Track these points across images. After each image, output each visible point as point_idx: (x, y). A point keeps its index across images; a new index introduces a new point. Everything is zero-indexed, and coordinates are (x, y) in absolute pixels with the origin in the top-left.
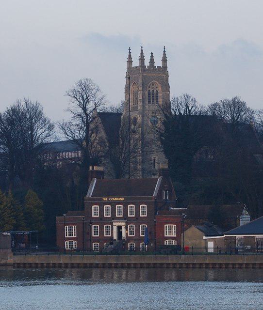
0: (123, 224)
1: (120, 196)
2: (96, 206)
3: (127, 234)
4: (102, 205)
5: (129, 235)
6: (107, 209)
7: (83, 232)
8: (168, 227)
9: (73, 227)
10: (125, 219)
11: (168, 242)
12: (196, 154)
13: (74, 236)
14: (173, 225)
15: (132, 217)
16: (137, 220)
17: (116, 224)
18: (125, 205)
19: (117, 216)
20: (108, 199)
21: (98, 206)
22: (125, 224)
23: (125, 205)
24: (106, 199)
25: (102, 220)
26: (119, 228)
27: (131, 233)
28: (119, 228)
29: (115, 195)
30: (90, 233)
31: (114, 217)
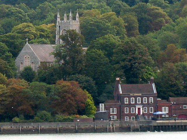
0: (141, 107)
1: (139, 93)
2: (151, 98)
3: (143, 112)
4: (129, 97)
5: (144, 113)
6: (126, 102)
7: (120, 111)
8: (164, 109)
9: (115, 108)
10: (142, 104)
11: (164, 116)
12: (153, 60)
13: (115, 113)
14: (167, 107)
15: (133, 104)
16: (148, 105)
17: (137, 107)
18: (142, 97)
19: (138, 103)
20: (133, 94)
21: (128, 98)
22: (142, 107)
23: (142, 97)
24: (132, 95)
25: (130, 105)
26: (139, 109)
27: (145, 111)
28: (139, 109)
29: (135, 92)
30: (123, 112)
31: (136, 103)
